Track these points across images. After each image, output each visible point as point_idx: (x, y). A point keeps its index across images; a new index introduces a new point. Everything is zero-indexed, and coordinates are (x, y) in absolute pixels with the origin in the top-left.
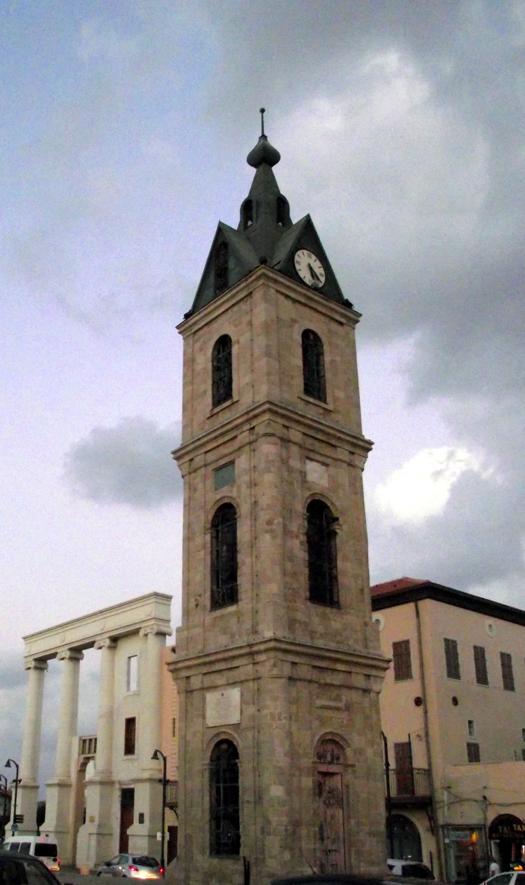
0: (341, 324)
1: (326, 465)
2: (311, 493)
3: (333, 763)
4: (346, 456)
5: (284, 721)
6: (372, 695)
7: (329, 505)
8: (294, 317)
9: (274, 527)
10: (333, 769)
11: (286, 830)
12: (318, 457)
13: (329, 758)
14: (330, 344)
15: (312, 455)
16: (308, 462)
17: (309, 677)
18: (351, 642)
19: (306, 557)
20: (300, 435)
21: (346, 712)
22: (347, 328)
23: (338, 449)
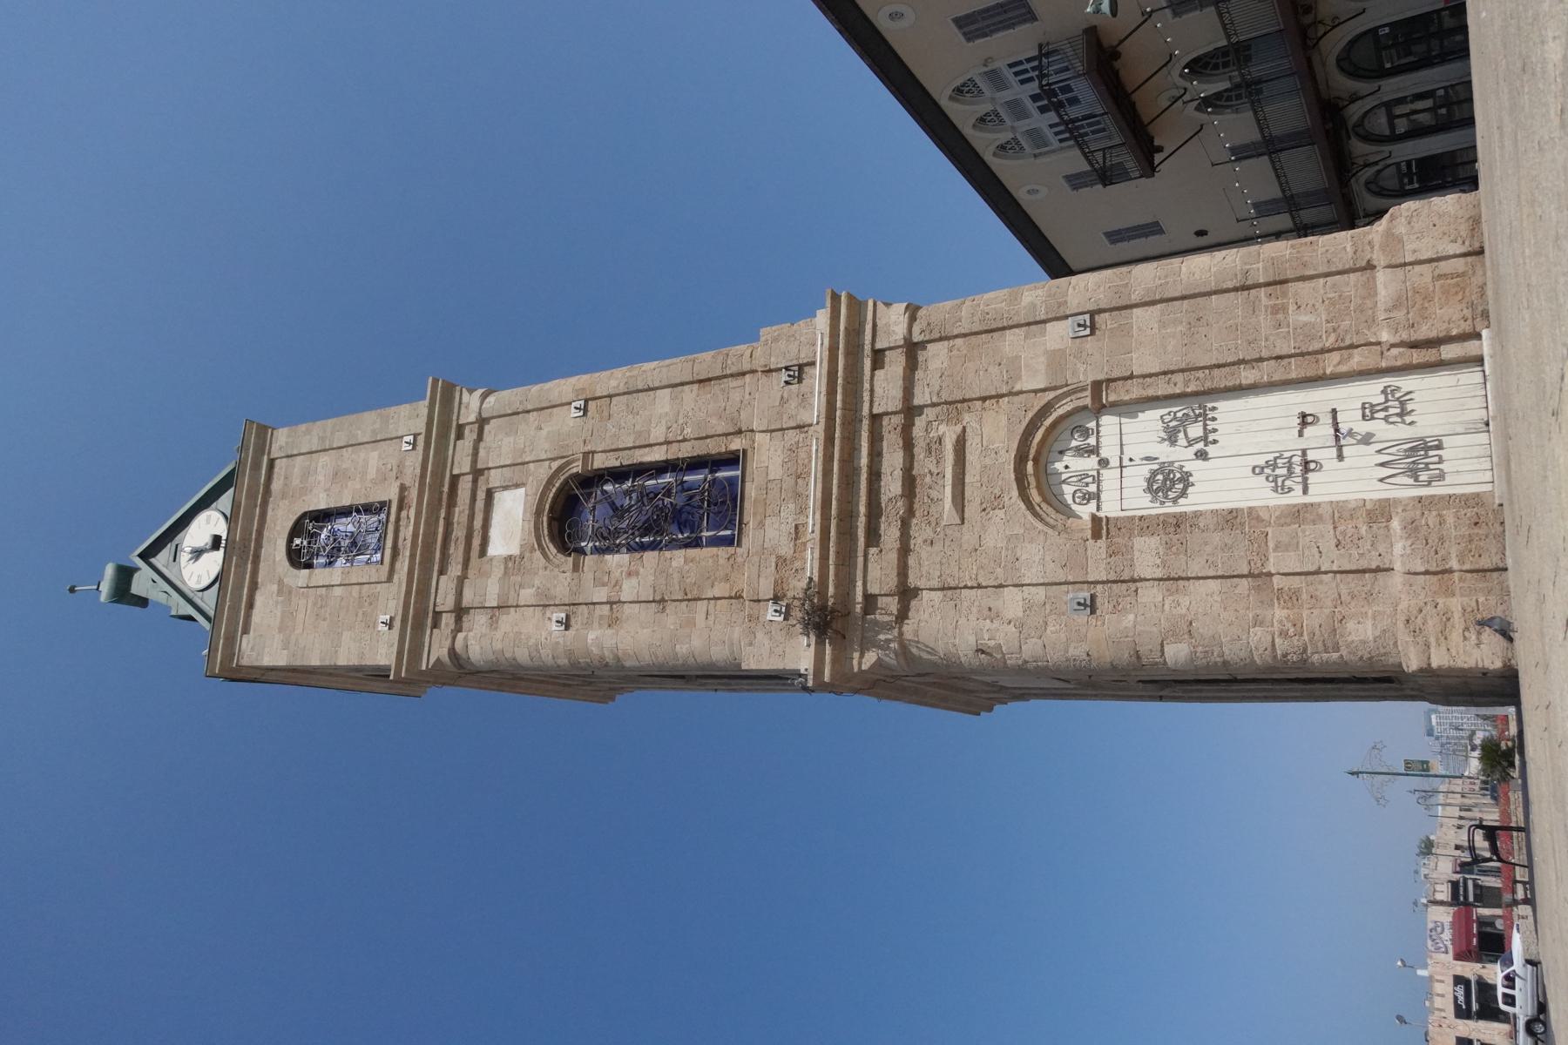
1: (490, 494)
4: (466, 445)
8: (275, 587)
12: (478, 523)
14: (304, 491)
15: (476, 542)
16: (492, 550)
20: (443, 578)
21: (967, 417)
23: (456, 472)
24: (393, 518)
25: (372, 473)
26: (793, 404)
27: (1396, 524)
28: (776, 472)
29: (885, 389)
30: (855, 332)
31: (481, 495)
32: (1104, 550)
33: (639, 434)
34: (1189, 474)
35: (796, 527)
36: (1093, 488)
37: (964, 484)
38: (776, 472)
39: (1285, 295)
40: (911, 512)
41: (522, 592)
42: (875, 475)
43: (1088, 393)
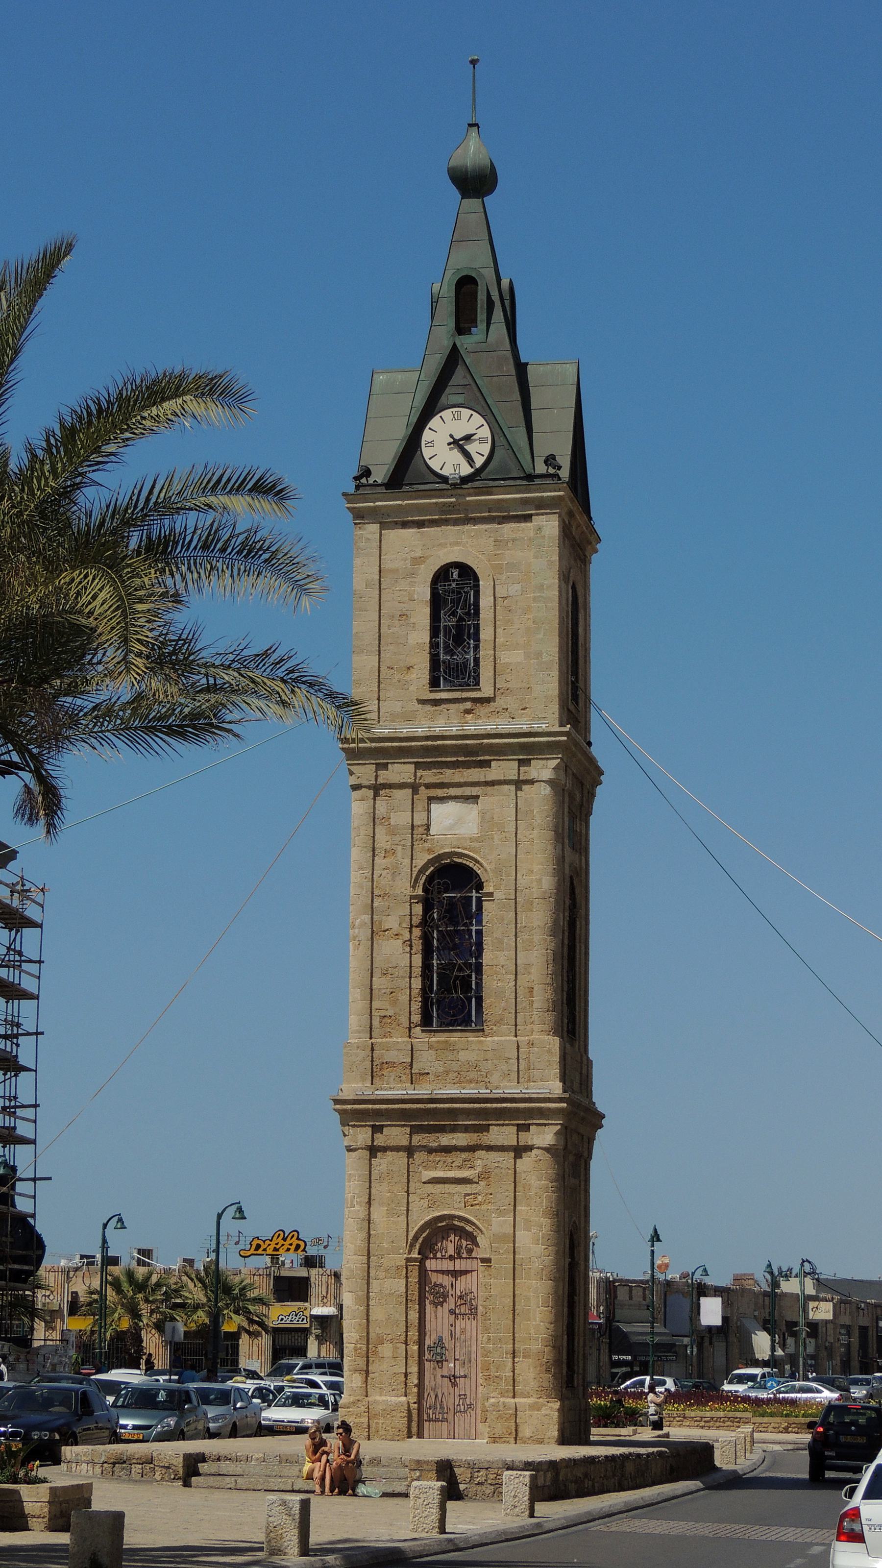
0: (527, 518)
2: (431, 857)
3: (461, 1258)
5: (357, 1208)
6: (535, 1152)
7: (471, 865)
8: (419, 554)
9: (356, 931)
10: (460, 1265)
11: (356, 1349)
13: (451, 1251)
15: (440, 793)
17: (405, 1143)
18: (495, 1078)
19: (418, 960)
22: (538, 521)
24: (465, 695)
25: (505, 657)
26: (505, 1067)
27: (404, 1399)
28: (463, 1056)
29: (502, 1134)
30: (542, 1113)
31: (474, 791)
32: (400, 1263)
33: (501, 942)
34: (442, 1306)
35: (428, 1074)
36: (439, 1255)
37: (445, 1183)
38: (463, 1056)
39: (524, 1357)
40: (431, 1151)
41: (400, 848)
42: (454, 1129)
43: (488, 1256)
